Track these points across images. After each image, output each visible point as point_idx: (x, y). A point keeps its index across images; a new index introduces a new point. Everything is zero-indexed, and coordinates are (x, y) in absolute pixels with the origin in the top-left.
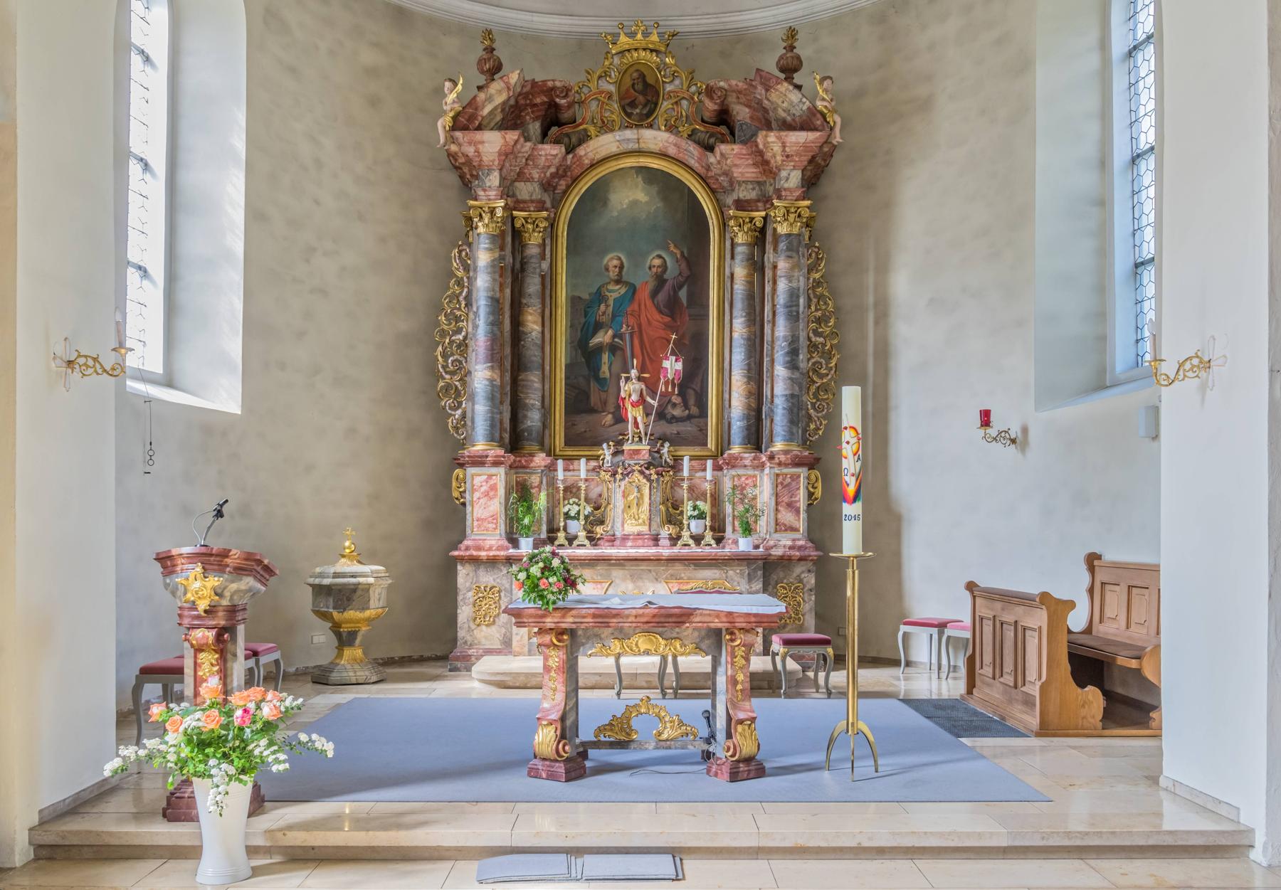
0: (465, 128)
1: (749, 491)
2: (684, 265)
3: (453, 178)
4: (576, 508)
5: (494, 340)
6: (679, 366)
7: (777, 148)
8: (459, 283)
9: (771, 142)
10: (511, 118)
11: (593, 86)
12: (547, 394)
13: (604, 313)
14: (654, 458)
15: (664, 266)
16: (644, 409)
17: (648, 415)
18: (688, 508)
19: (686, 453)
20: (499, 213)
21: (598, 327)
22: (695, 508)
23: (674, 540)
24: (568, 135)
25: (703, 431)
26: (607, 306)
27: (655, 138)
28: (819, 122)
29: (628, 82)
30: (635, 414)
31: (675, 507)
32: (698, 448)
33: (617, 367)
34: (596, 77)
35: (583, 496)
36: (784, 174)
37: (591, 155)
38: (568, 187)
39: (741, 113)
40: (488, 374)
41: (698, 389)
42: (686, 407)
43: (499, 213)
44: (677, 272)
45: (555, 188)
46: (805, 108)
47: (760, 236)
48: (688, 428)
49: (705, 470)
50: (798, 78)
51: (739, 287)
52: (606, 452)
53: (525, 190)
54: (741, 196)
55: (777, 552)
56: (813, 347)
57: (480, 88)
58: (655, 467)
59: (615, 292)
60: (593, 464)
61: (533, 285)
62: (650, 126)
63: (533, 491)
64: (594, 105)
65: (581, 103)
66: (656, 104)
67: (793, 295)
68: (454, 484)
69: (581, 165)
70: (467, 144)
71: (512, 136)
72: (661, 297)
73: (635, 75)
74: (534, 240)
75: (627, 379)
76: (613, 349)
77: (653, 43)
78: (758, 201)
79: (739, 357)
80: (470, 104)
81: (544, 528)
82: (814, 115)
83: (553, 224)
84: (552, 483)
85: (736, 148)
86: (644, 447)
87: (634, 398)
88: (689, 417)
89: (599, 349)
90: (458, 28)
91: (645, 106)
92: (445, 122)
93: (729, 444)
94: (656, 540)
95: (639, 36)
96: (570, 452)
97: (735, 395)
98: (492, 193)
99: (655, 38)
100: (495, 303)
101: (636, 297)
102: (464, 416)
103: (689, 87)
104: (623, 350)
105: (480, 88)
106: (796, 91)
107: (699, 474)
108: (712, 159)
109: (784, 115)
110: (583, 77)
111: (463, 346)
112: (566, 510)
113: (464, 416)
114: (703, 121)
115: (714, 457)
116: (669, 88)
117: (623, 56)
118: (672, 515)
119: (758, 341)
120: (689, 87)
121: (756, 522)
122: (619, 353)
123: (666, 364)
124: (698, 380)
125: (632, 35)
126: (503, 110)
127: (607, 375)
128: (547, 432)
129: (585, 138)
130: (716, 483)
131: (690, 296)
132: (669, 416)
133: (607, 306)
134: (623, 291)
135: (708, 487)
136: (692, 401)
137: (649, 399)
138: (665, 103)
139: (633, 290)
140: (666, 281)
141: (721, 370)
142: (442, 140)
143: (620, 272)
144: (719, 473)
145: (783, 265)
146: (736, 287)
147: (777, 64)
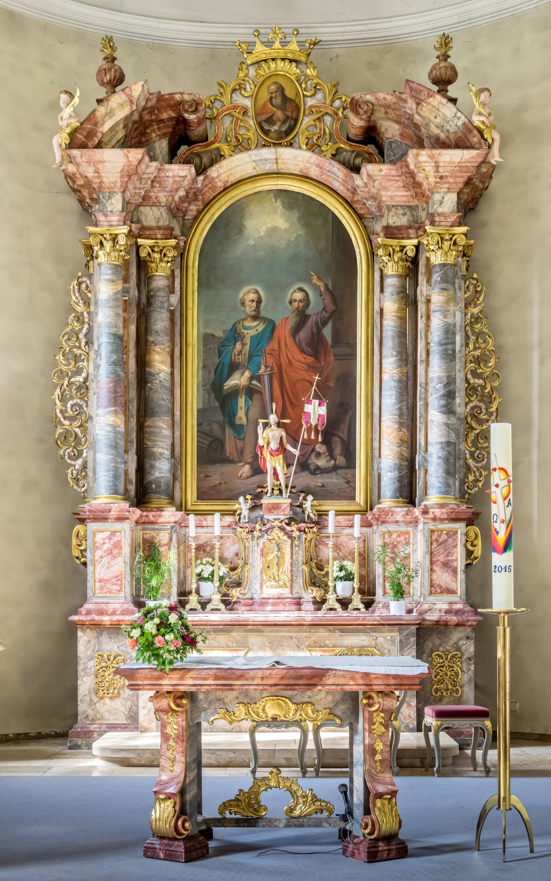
0: (83, 146)
1: (402, 551)
2: (328, 299)
3: (71, 202)
4: (210, 569)
5: (118, 381)
6: (323, 410)
7: (429, 168)
8: (79, 318)
9: (422, 160)
10: (136, 134)
11: (226, 100)
12: (177, 442)
13: (240, 352)
14: (295, 513)
15: (306, 301)
16: (285, 458)
17: (289, 465)
18: (333, 570)
19: (331, 507)
20: (122, 240)
21: (233, 367)
22: (341, 569)
23: (319, 604)
24: (198, 155)
25: (351, 483)
26: (243, 345)
27: (296, 158)
28: (475, 140)
29: (264, 96)
30: (273, 463)
31: (320, 568)
32: (345, 502)
33: (255, 410)
34: (229, 90)
35: (217, 555)
36: (437, 197)
37: (224, 177)
38: (200, 212)
39: (390, 130)
40: (111, 419)
41: (344, 436)
42: (332, 456)
43: (122, 240)
44: (322, 307)
45: (185, 213)
46: (460, 123)
47: (412, 267)
48: (333, 480)
49: (352, 526)
50: (452, 90)
51: (390, 323)
52: (243, 505)
53: (152, 216)
54: (391, 222)
55: (432, 617)
56: (471, 390)
57: (99, 101)
58: (297, 522)
59: (253, 329)
60: (229, 519)
61: (160, 321)
62: (290, 145)
63: (162, 549)
64: (227, 121)
65: (213, 119)
66: (296, 120)
67: (449, 332)
68: (74, 541)
69: (214, 188)
70: (85, 162)
71: (136, 154)
72: (303, 334)
73: (273, 88)
74: (161, 271)
75: (266, 425)
76: (250, 392)
77: (292, 52)
78: (410, 227)
79: (390, 401)
80: (88, 119)
81: (174, 590)
82: (470, 131)
83: (182, 255)
84: (183, 541)
85: (385, 168)
86: (285, 501)
87: (274, 445)
88: (335, 468)
89: (235, 392)
90: (75, 36)
91: (284, 122)
92: (62, 138)
93: (379, 497)
94: (298, 603)
95: (277, 45)
96: (204, 506)
97: (385, 443)
98: (115, 219)
99: (294, 46)
100: (119, 340)
101: (276, 334)
102: (84, 467)
103: (333, 101)
104: (261, 393)
105: (99, 101)
106: (450, 105)
107: (347, 531)
108: (358, 180)
109: (436, 131)
110: (215, 90)
111: (84, 388)
112: (198, 570)
113: (84, 467)
114: (349, 139)
115: (363, 512)
116: (310, 102)
117: (260, 67)
118: (317, 580)
119: (410, 383)
120: (333, 101)
121: (409, 583)
122: (256, 397)
123: (308, 408)
124: (344, 427)
125: (269, 44)
126: (125, 126)
127: (244, 421)
128: (177, 484)
129: (218, 157)
130: (365, 540)
131: (336, 333)
132: (312, 467)
133: (243, 345)
134: (261, 327)
135: (355, 545)
136: (338, 450)
137: (289, 447)
138: (306, 120)
139: (272, 326)
140: (308, 317)
141: (370, 416)
142: (58, 159)
143: (258, 307)
144: (369, 530)
145: (437, 298)
146: (385, 323)
147: (429, 77)
